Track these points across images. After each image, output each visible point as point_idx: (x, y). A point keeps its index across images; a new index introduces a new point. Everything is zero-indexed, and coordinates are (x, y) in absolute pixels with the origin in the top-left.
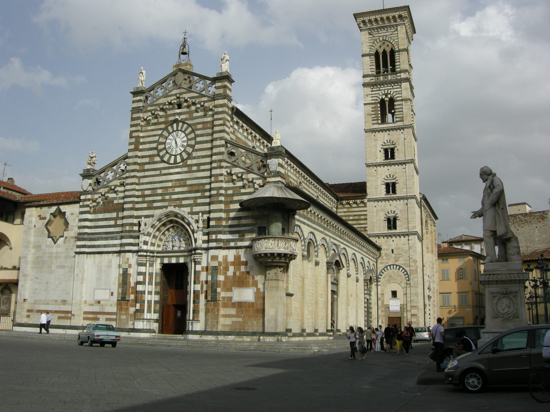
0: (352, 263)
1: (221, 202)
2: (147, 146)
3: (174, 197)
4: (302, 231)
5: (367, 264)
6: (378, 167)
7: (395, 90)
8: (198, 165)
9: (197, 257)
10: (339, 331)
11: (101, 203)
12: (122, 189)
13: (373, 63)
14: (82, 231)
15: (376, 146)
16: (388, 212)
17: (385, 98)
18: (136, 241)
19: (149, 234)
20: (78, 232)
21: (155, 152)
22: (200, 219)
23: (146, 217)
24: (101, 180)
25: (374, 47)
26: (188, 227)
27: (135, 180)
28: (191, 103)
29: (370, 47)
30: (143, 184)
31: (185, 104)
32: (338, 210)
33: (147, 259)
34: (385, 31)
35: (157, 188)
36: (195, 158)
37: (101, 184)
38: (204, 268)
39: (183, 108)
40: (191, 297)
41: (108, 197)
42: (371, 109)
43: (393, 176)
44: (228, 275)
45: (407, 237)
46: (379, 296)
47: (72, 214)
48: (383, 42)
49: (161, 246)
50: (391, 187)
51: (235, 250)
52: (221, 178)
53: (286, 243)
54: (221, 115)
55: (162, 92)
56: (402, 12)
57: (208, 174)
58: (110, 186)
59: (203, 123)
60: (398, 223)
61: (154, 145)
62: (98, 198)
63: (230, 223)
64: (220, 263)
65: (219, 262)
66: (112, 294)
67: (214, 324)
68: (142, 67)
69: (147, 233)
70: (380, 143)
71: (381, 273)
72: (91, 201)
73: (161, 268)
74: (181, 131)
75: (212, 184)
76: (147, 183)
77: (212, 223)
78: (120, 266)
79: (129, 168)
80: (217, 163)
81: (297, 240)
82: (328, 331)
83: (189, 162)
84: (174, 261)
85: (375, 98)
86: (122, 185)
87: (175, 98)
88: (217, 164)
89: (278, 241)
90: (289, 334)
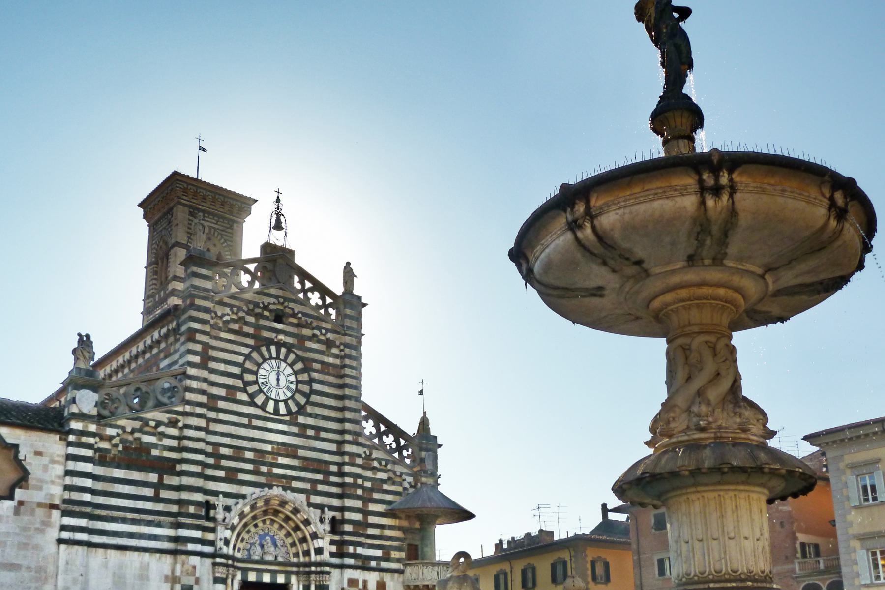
1: (359, 497)
2: (222, 367)
3: (276, 471)
8: (318, 429)
11: (120, 448)
12: (174, 432)
14: (75, 496)
19: (233, 528)
21: (239, 383)
22: (327, 517)
26: (303, 527)
27: (202, 423)
30: (215, 433)
36: (310, 415)
39: (287, 325)
41: (139, 439)
47: (38, 454)
52: (359, 461)
57: (333, 447)
58: (145, 418)
59: (322, 363)
61: (236, 370)
74: (285, 361)
83: (301, 420)
86: (173, 424)
88: (353, 438)
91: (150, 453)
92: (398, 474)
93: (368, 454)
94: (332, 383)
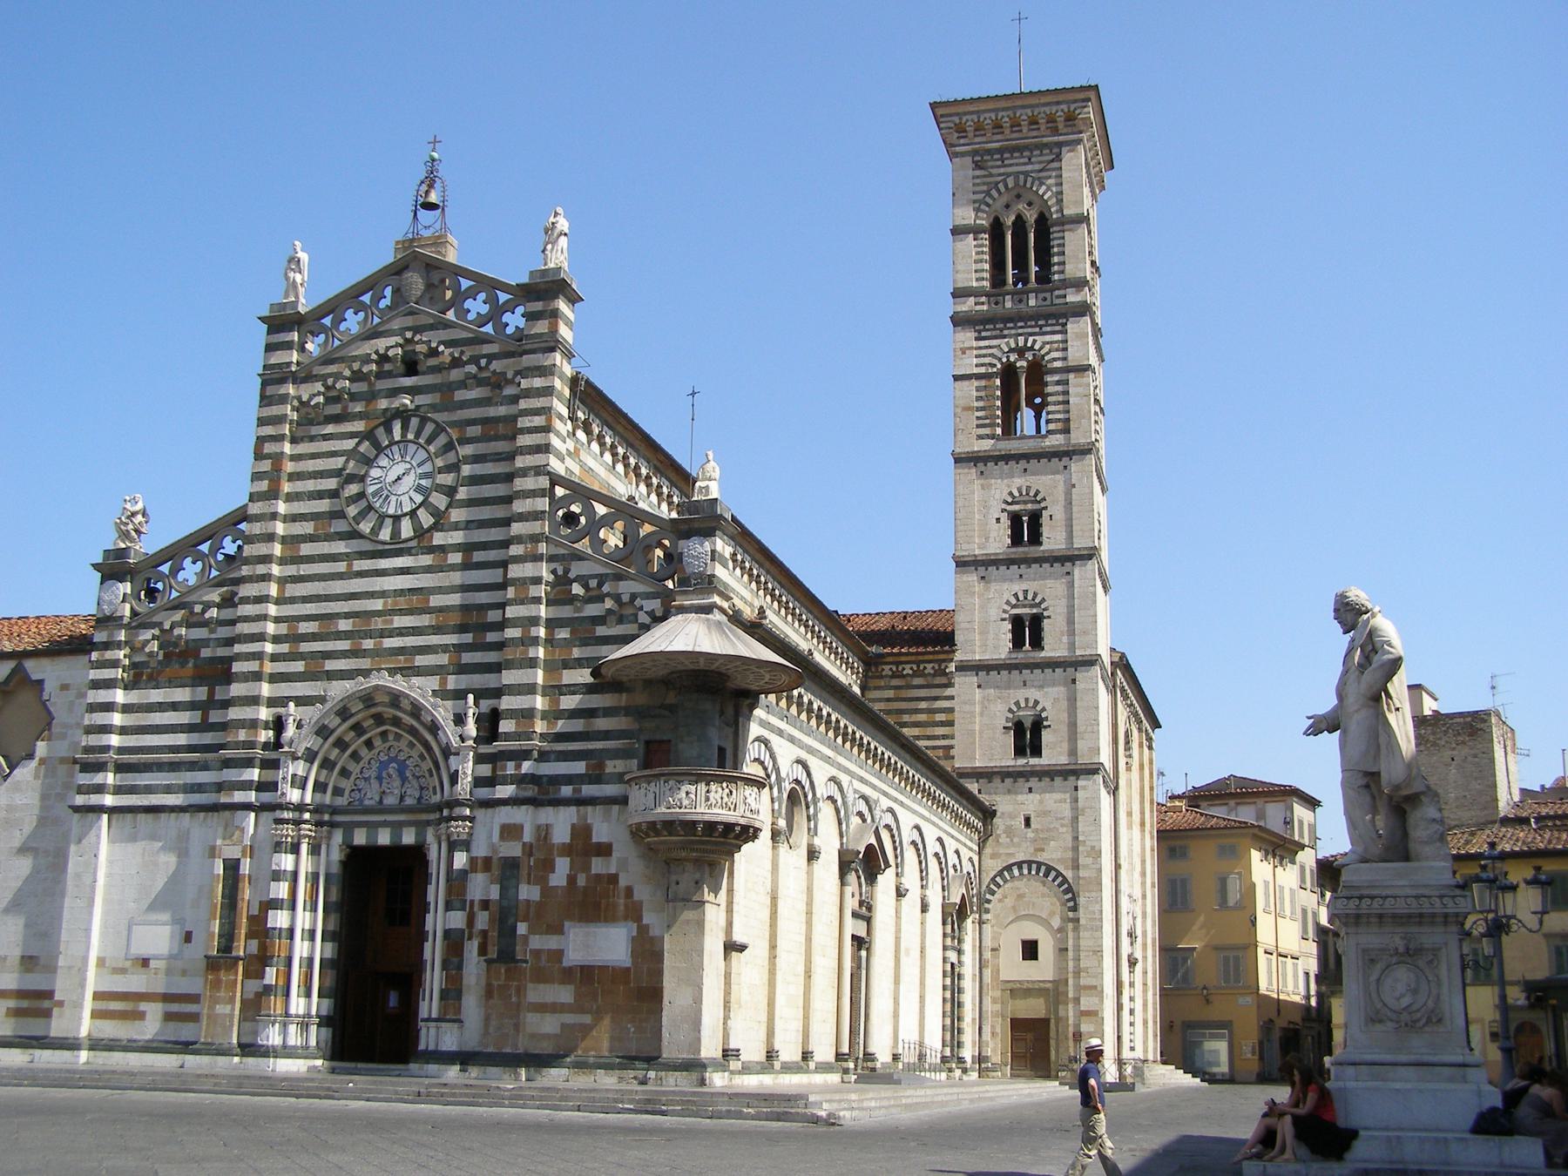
0: (910, 855)
2: (310, 485)
3: (389, 643)
4: (773, 756)
5: (952, 859)
6: (990, 568)
7: (1048, 338)
9: (457, 827)
10: (869, 1057)
11: (161, 657)
12: (227, 614)
13: (982, 252)
14: (94, 740)
15: (985, 505)
16: (1017, 704)
17: (1017, 360)
18: (269, 775)
19: (310, 756)
20: (84, 744)
23: (301, 701)
24: (160, 586)
25: (988, 205)
26: (429, 737)
28: (448, 360)
29: (977, 205)
31: (432, 362)
32: (867, 692)
33: (302, 832)
34: (1022, 160)
35: (337, 614)
37: (161, 601)
38: (479, 861)
39: (424, 373)
40: (433, 951)
42: (975, 394)
43: (1035, 595)
44: (552, 883)
45: (1072, 778)
46: (988, 955)
47: (64, 687)
48: (1015, 193)
49: (347, 793)
50: (1027, 629)
51: (573, 809)
53: (731, 792)
54: (541, 399)
55: (358, 323)
56: (1076, 105)
59: (485, 421)
60: (1046, 736)
61: (331, 484)
62: (148, 641)
63: (561, 726)
64: (529, 849)
65: (524, 844)
66: (188, 937)
67: (507, 1031)
68: (297, 243)
69: (302, 750)
70: (997, 497)
71: (992, 886)
72: (127, 651)
73: (343, 858)
75: (508, 608)
76: (306, 600)
77: (506, 726)
78: (217, 852)
79: (248, 550)
80: (526, 543)
81: (759, 784)
82: (839, 1056)
83: (438, 539)
84: (384, 838)
85: (987, 360)
87: (401, 341)
89: (708, 784)
90: (734, 1065)
91: (196, 654)
92: (625, 598)
93: (560, 572)
94: (500, 454)
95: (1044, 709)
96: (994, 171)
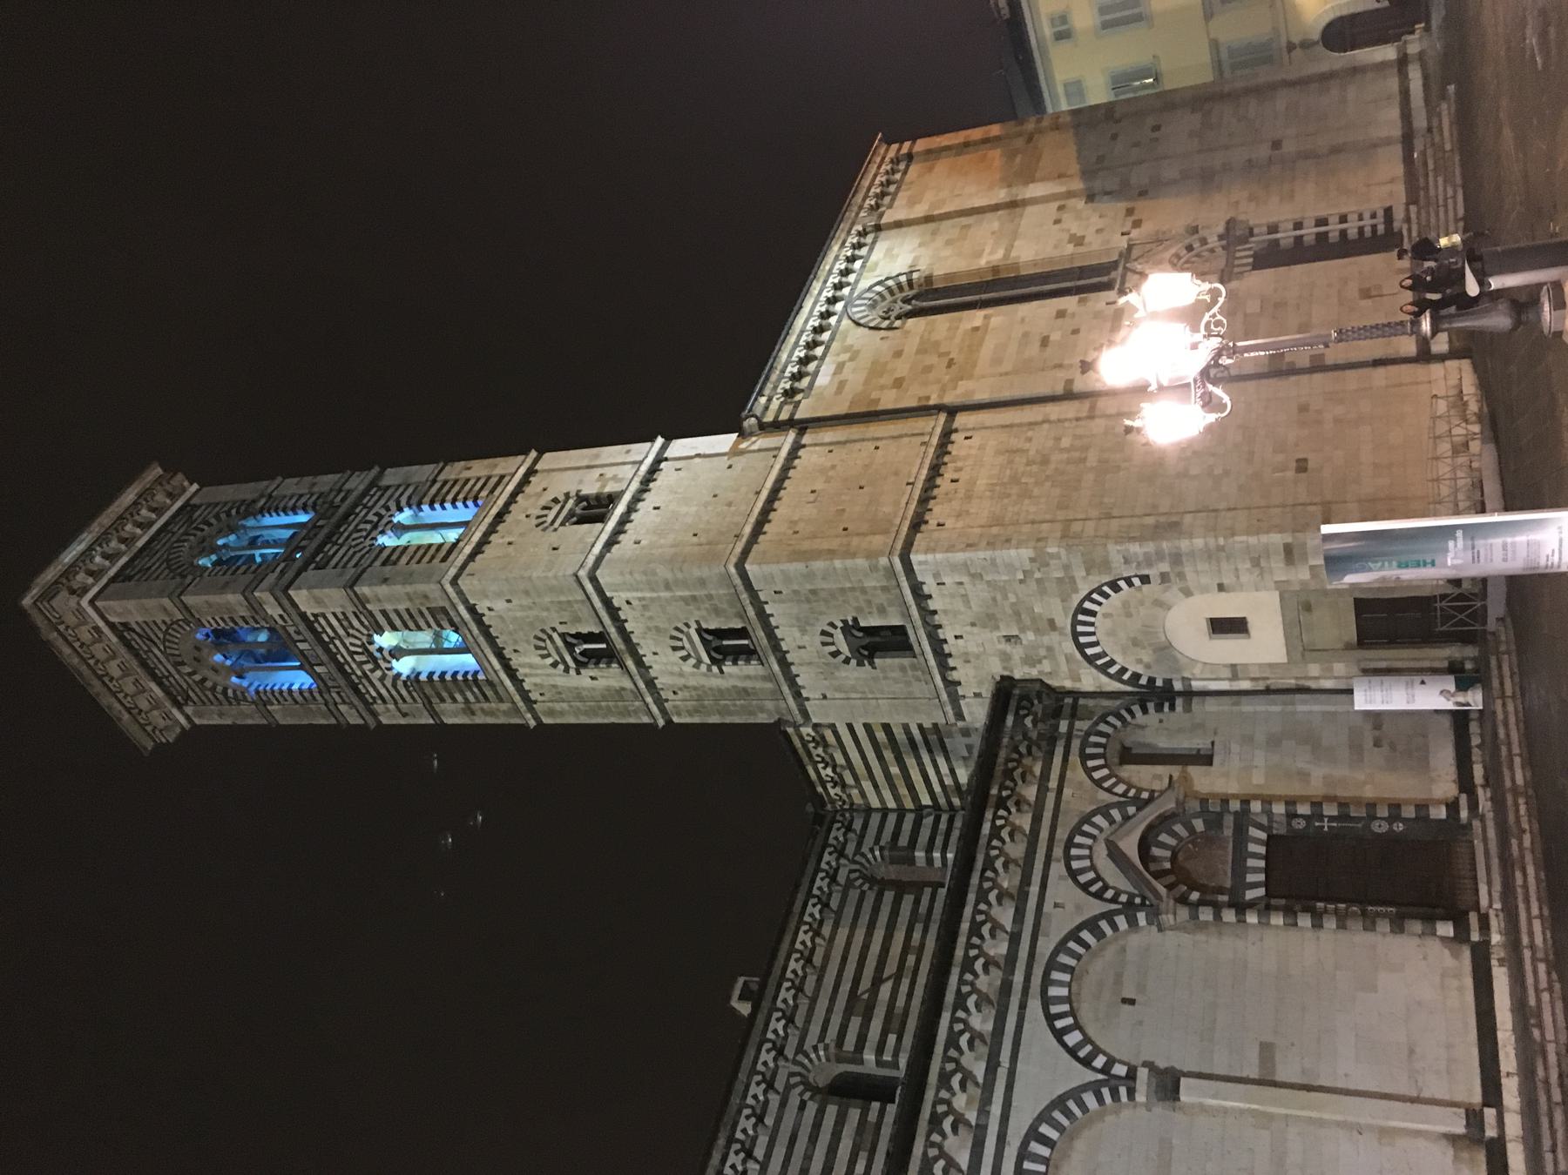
95: (832, 625)
96: (185, 686)
